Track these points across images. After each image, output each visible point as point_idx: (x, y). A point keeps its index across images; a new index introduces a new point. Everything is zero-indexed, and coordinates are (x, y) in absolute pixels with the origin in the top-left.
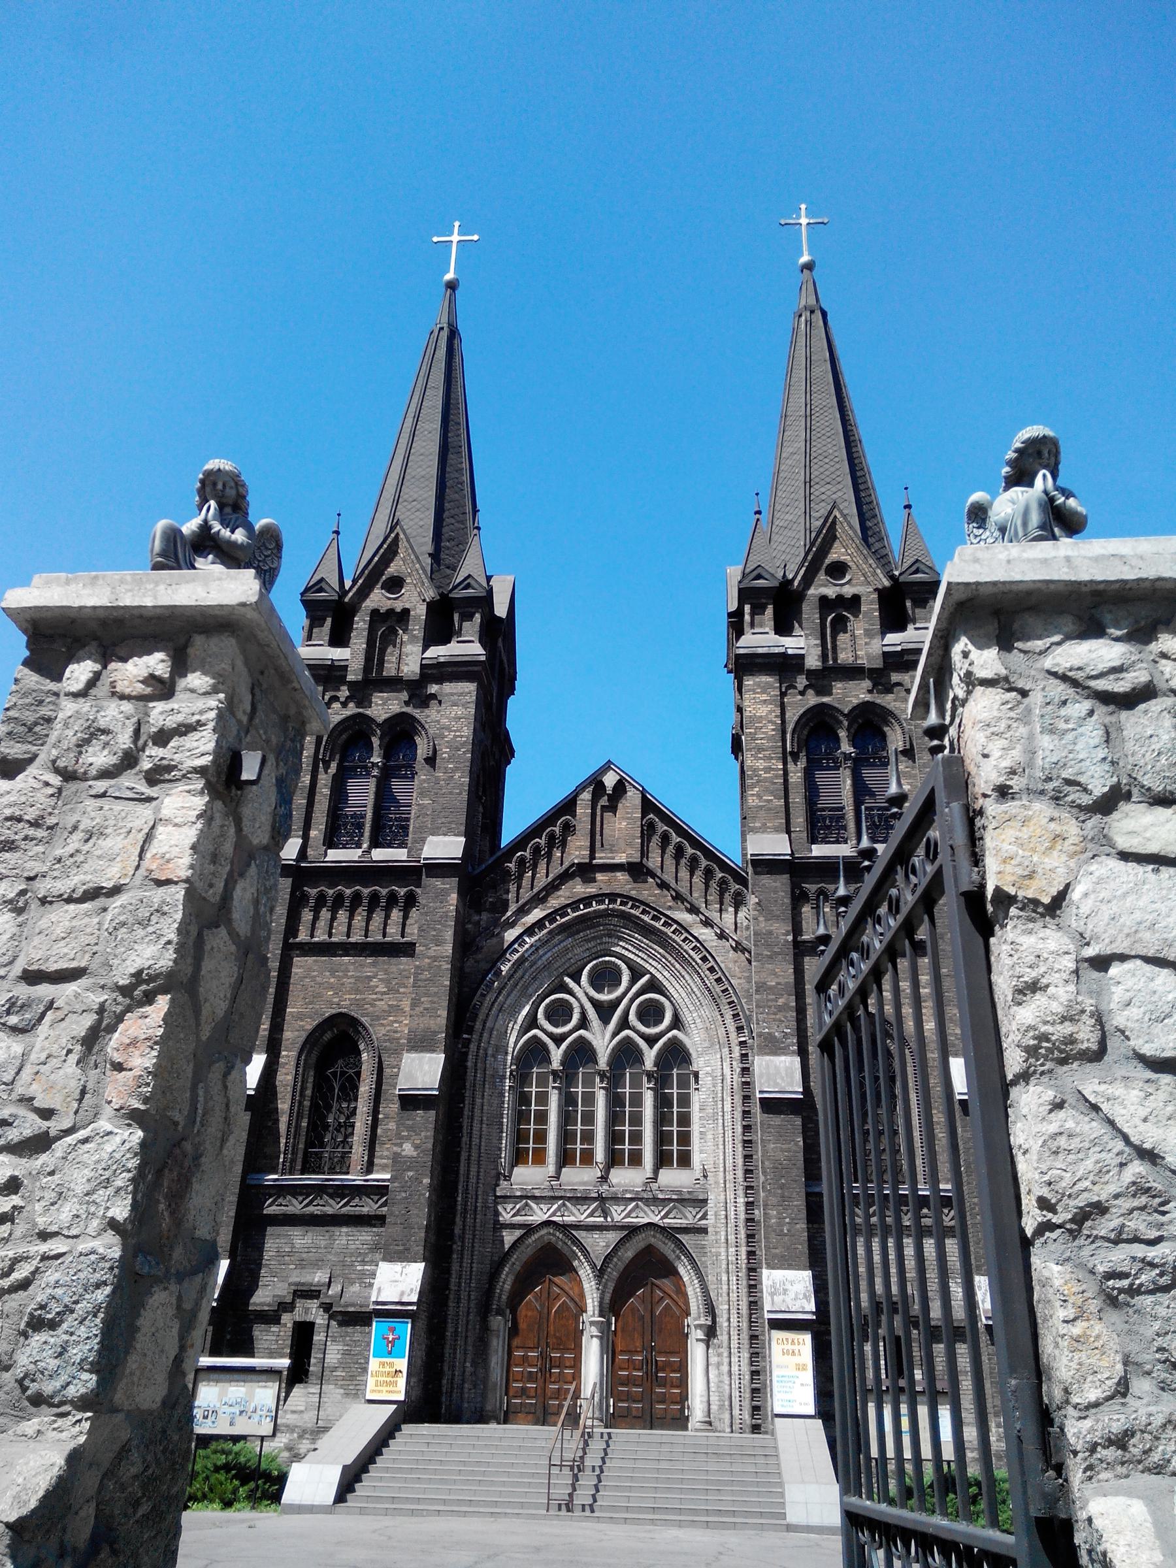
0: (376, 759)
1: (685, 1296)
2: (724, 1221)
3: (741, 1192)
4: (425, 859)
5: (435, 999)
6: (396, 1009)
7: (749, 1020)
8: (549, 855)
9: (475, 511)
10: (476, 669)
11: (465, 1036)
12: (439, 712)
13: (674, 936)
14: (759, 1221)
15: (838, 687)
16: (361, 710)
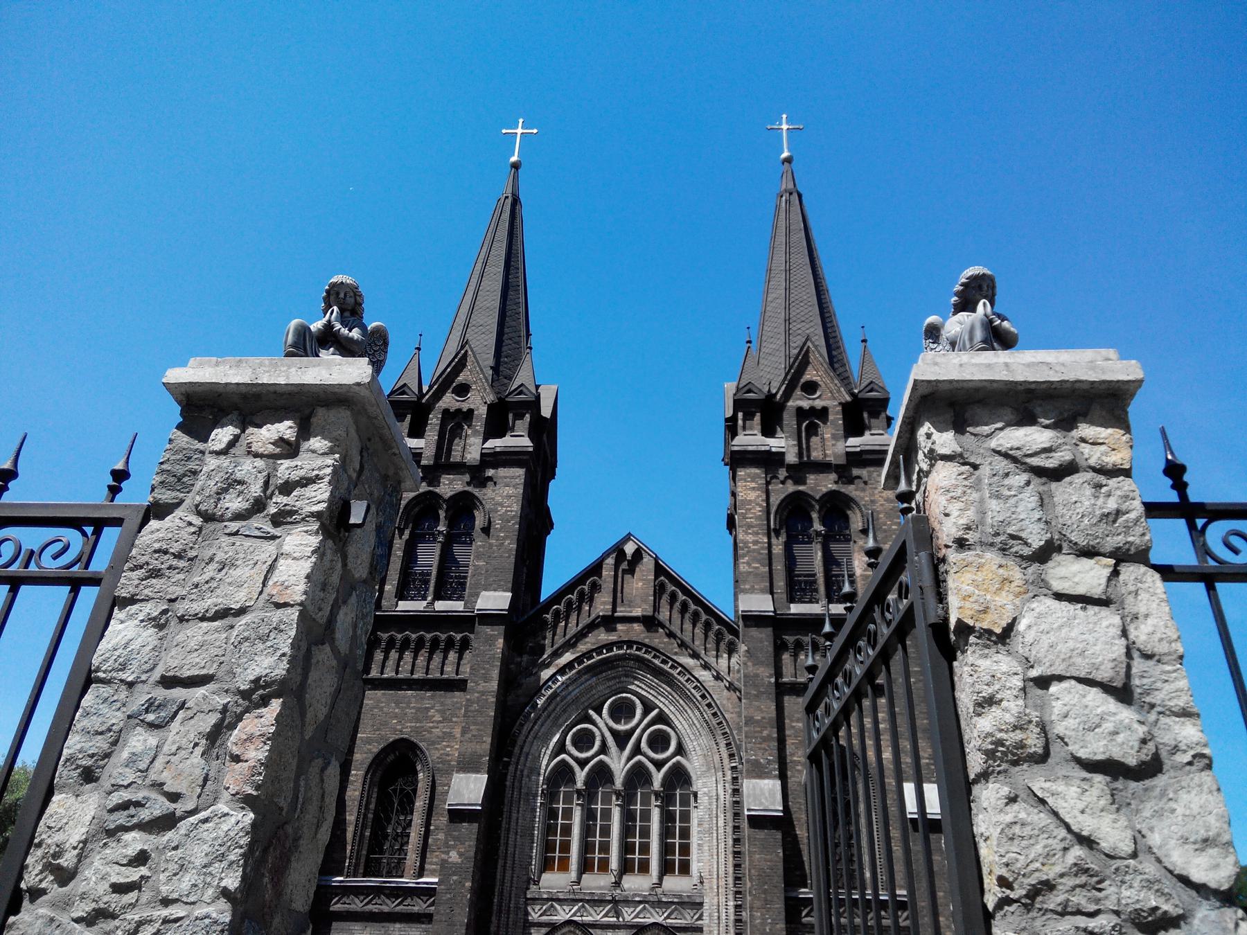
0: (442, 528)
2: (716, 922)
3: (731, 897)
4: (478, 610)
5: (482, 728)
6: (449, 736)
7: (739, 748)
8: (579, 609)
9: (528, 335)
10: (525, 457)
11: (505, 759)
12: (494, 491)
13: (679, 677)
14: (746, 922)
15: (811, 479)
16: (431, 489)
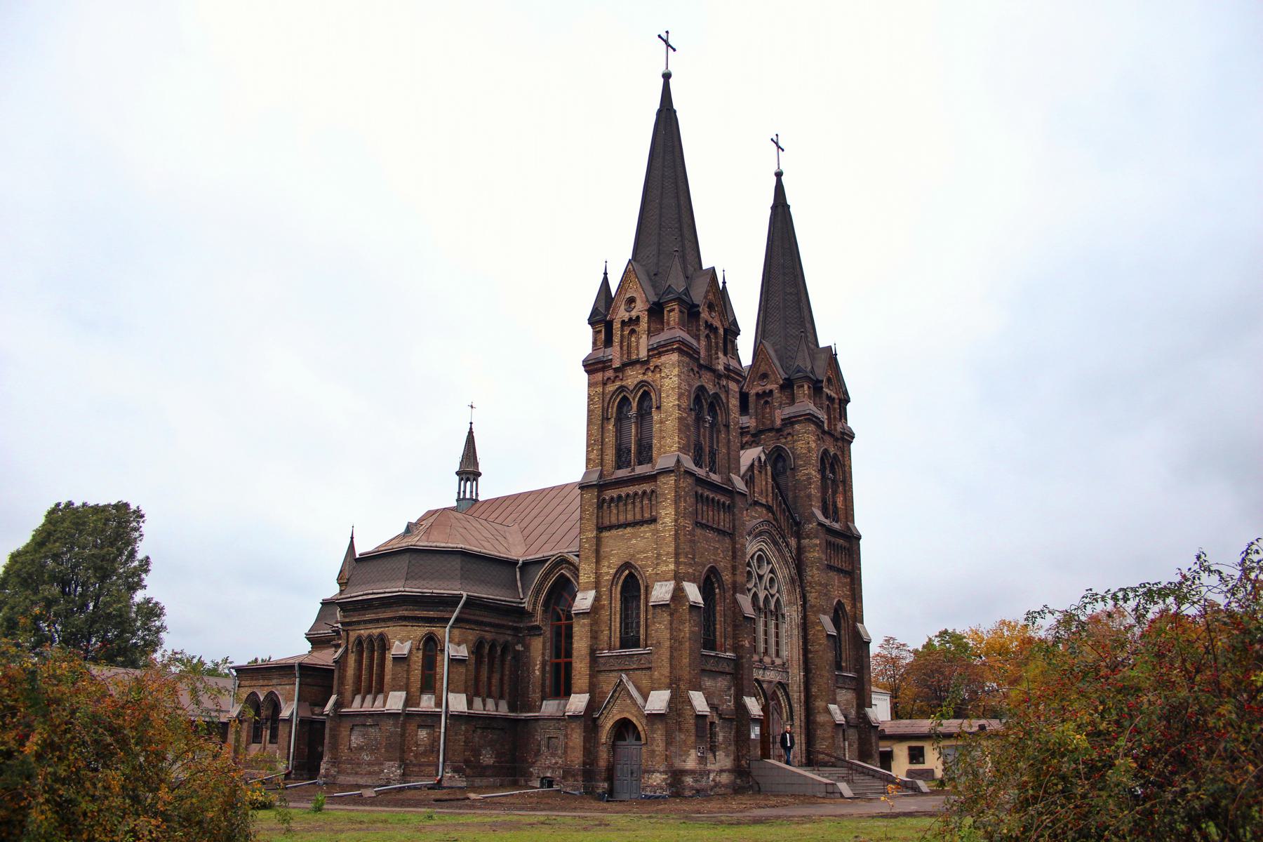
1: (781, 712)
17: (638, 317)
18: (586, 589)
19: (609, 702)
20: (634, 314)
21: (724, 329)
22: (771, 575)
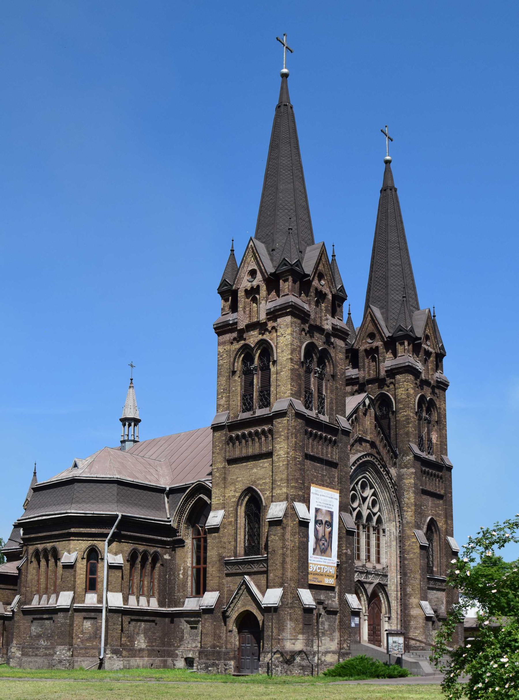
3: (399, 574)
17: (258, 286)
18: (217, 509)
19: (234, 598)
20: (255, 283)
21: (332, 295)
22: (373, 497)
